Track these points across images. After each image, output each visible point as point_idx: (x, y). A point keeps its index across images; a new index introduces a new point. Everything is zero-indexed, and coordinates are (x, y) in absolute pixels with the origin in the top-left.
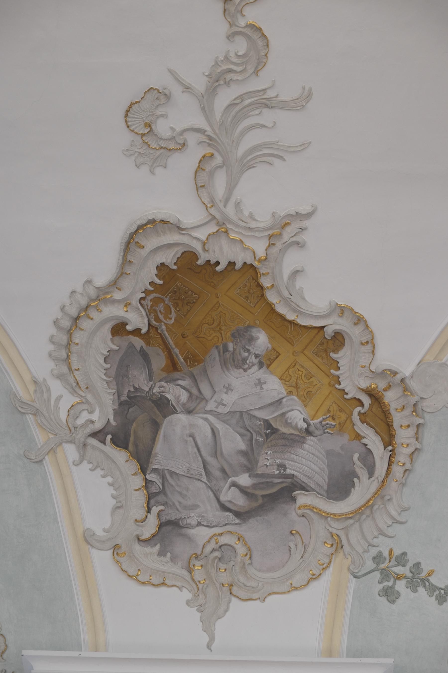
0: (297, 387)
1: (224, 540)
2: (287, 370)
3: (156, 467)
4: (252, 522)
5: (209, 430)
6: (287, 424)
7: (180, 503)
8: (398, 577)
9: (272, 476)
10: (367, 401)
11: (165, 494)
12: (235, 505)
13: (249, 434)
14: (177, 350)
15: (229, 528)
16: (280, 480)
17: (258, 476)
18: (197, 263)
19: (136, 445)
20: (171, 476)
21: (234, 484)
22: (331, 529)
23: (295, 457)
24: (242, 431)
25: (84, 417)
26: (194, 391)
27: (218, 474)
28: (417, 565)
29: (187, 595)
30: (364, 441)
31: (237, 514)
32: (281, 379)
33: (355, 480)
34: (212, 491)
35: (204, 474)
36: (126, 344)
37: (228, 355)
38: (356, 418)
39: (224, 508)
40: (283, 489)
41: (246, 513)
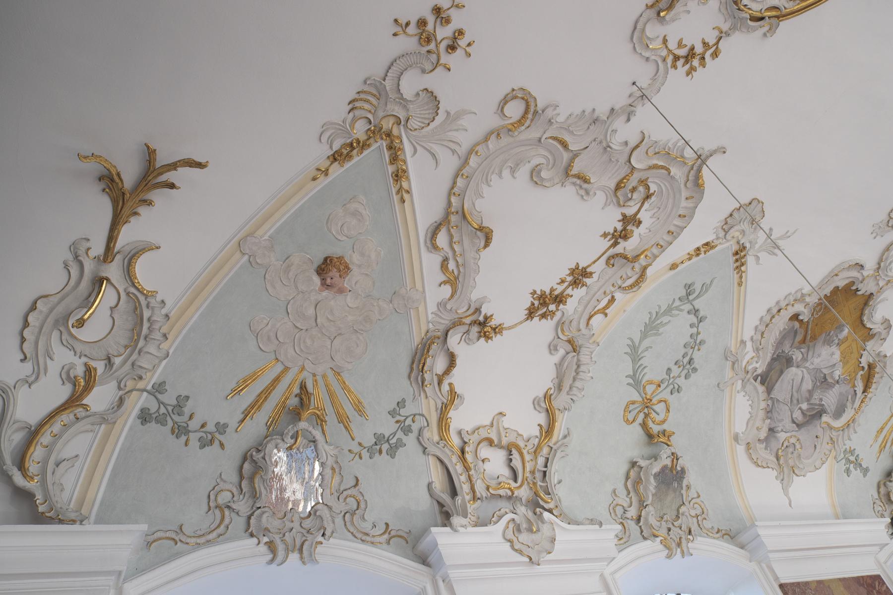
0: (844, 358)
1: (793, 440)
2: (846, 349)
3: (772, 396)
4: (803, 430)
5: (801, 377)
6: (832, 377)
7: (777, 418)
8: (852, 462)
9: (815, 404)
10: (866, 367)
11: (772, 413)
12: (798, 420)
13: (815, 381)
14: (810, 332)
15: (794, 433)
16: (818, 407)
17: (812, 404)
18: (852, 288)
19: (768, 384)
20: (777, 402)
21: (800, 409)
22: (831, 435)
23: (828, 395)
24: (814, 379)
25: (754, 365)
26: (805, 356)
27: (795, 402)
28: (857, 456)
29: (775, 473)
30: (856, 389)
31: (798, 425)
32: (841, 353)
33: (846, 409)
34: (791, 412)
35: (790, 401)
36: (792, 325)
37: (828, 337)
38: (859, 376)
39: (794, 422)
40: (818, 412)
41: (802, 424)
